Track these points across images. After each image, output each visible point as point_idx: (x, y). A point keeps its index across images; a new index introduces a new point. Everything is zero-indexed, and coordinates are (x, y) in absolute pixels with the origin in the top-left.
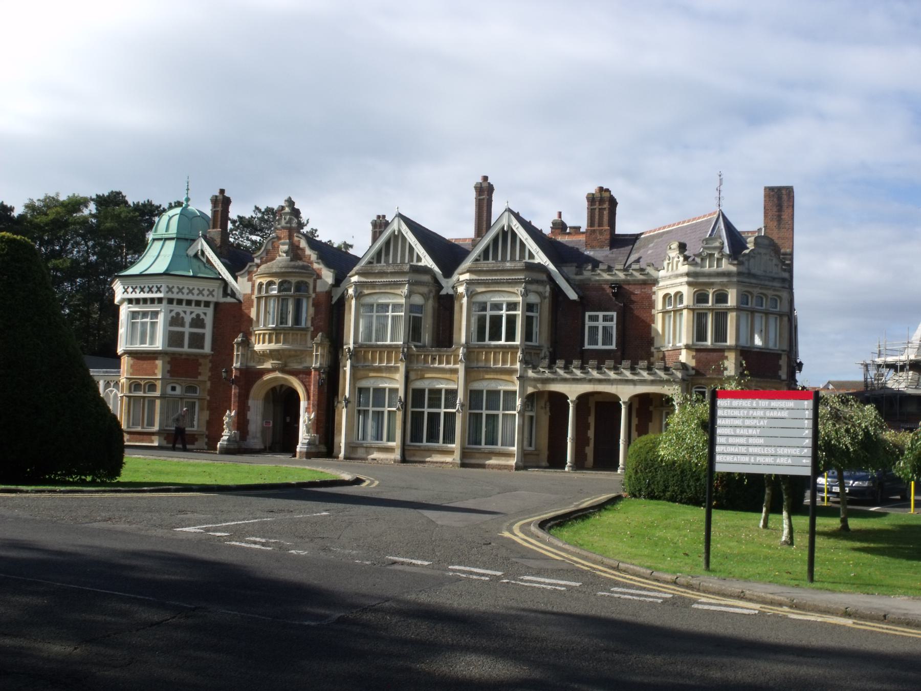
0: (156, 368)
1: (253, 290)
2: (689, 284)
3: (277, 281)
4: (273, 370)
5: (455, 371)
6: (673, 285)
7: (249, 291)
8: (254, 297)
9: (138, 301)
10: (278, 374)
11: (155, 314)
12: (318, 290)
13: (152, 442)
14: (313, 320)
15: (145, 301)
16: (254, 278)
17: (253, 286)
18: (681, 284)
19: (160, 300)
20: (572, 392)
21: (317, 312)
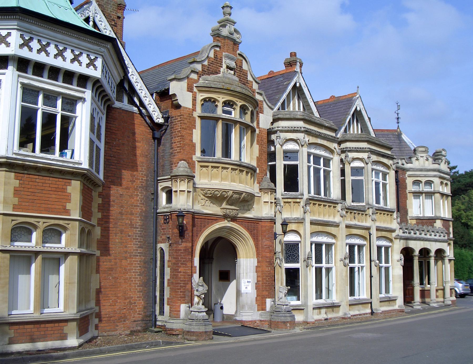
0: (68, 200)
1: (194, 105)
2: (441, 177)
3: (240, 103)
4: (225, 217)
5: (368, 229)
6: (425, 176)
7: (190, 106)
8: (196, 114)
9: (39, 68)
10: (226, 223)
11: (71, 103)
12: (260, 126)
13: (64, 337)
14: (259, 159)
15: (54, 72)
16: (195, 90)
17: (194, 100)
18: (435, 176)
19: (83, 80)
20: (417, 246)
21: (260, 154)
